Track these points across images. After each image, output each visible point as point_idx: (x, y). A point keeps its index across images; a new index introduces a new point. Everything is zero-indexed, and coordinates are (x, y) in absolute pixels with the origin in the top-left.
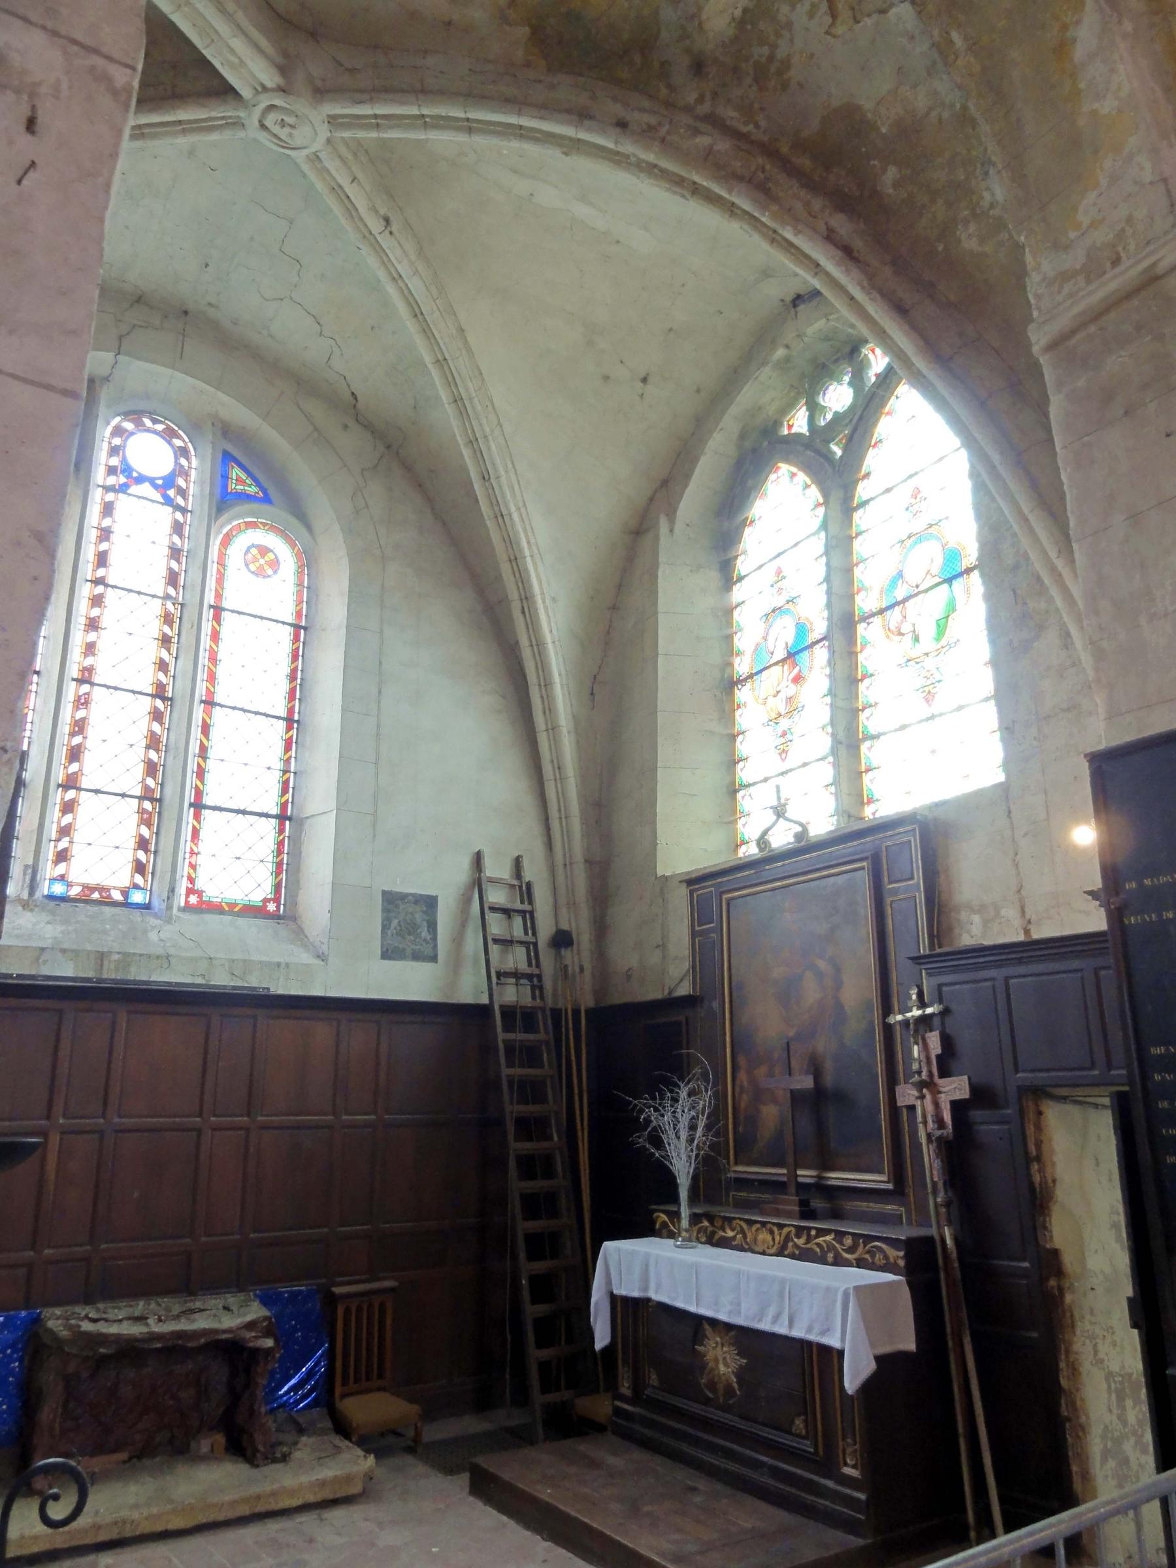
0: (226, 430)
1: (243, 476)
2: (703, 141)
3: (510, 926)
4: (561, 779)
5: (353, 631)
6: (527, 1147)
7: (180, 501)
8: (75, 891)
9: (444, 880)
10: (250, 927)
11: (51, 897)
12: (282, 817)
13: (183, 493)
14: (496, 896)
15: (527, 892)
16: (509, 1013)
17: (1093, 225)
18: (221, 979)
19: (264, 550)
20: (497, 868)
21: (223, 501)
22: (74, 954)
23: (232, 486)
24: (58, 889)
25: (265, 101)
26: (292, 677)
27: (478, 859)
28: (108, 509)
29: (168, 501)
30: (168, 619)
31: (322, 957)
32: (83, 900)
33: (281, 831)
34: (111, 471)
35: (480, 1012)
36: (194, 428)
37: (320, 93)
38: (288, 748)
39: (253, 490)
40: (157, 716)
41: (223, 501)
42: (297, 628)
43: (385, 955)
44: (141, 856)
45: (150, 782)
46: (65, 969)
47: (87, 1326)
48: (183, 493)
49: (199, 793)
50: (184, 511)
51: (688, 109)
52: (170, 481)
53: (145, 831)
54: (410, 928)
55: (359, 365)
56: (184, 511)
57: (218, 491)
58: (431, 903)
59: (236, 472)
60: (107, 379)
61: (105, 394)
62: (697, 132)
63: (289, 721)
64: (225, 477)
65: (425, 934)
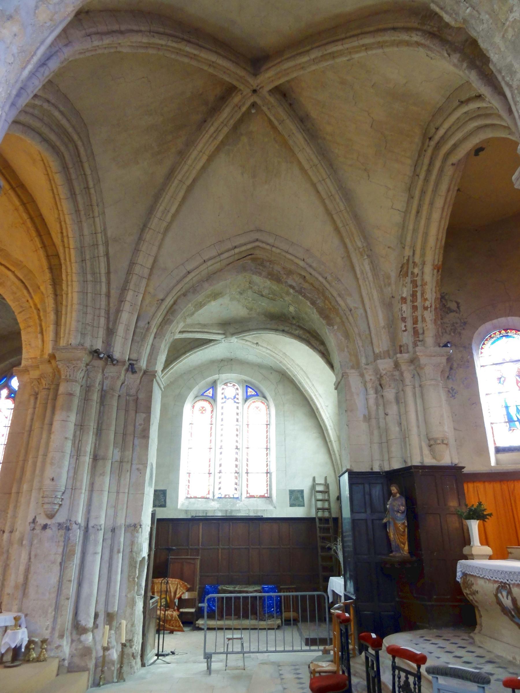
0: (245, 381)
1: (251, 390)
2: (297, 332)
3: (325, 497)
4: (335, 454)
5: (277, 425)
6: (324, 554)
7: (237, 401)
8: (223, 496)
9: (305, 485)
10: (260, 501)
11: (219, 498)
12: (267, 473)
13: (238, 399)
14: (318, 488)
15: (327, 485)
16: (320, 519)
18: (252, 514)
19: (257, 408)
20: (320, 480)
21: (247, 398)
22: (221, 511)
23: (249, 394)
24: (220, 496)
25: (223, 340)
26: (267, 438)
27: (314, 479)
28: (222, 408)
29: (235, 402)
30: (237, 430)
31: (275, 507)
32: (225, 498)
33: (267, 476)
34: (222, 399)
35: (314, 519)
36: (240, 382)
37: (233, 334)
38: (267, 455)
39: (254, 393)
40: (237, 453)
41: (247, 398)
42: (267, 425)
43: (292, 505)
44: (236, 486)
45: (237, 469)
46: (219, 514)
47: (224, 588)
48: (238, 399)
49: (247, 470)
50: (238, 403)
51: (294, 324)
52: (235, 397)
53: (236, 481)
54: (297, 498)
55: (268, 361)
56: (238, 403)
57: (245, 396)
58: (302, 492)
59: (249, 390)
60: (218, 379)
61: (218, 383)
62: (296, 330)
63: (267, 449)
64: (247, 392)
65: (301, 499)
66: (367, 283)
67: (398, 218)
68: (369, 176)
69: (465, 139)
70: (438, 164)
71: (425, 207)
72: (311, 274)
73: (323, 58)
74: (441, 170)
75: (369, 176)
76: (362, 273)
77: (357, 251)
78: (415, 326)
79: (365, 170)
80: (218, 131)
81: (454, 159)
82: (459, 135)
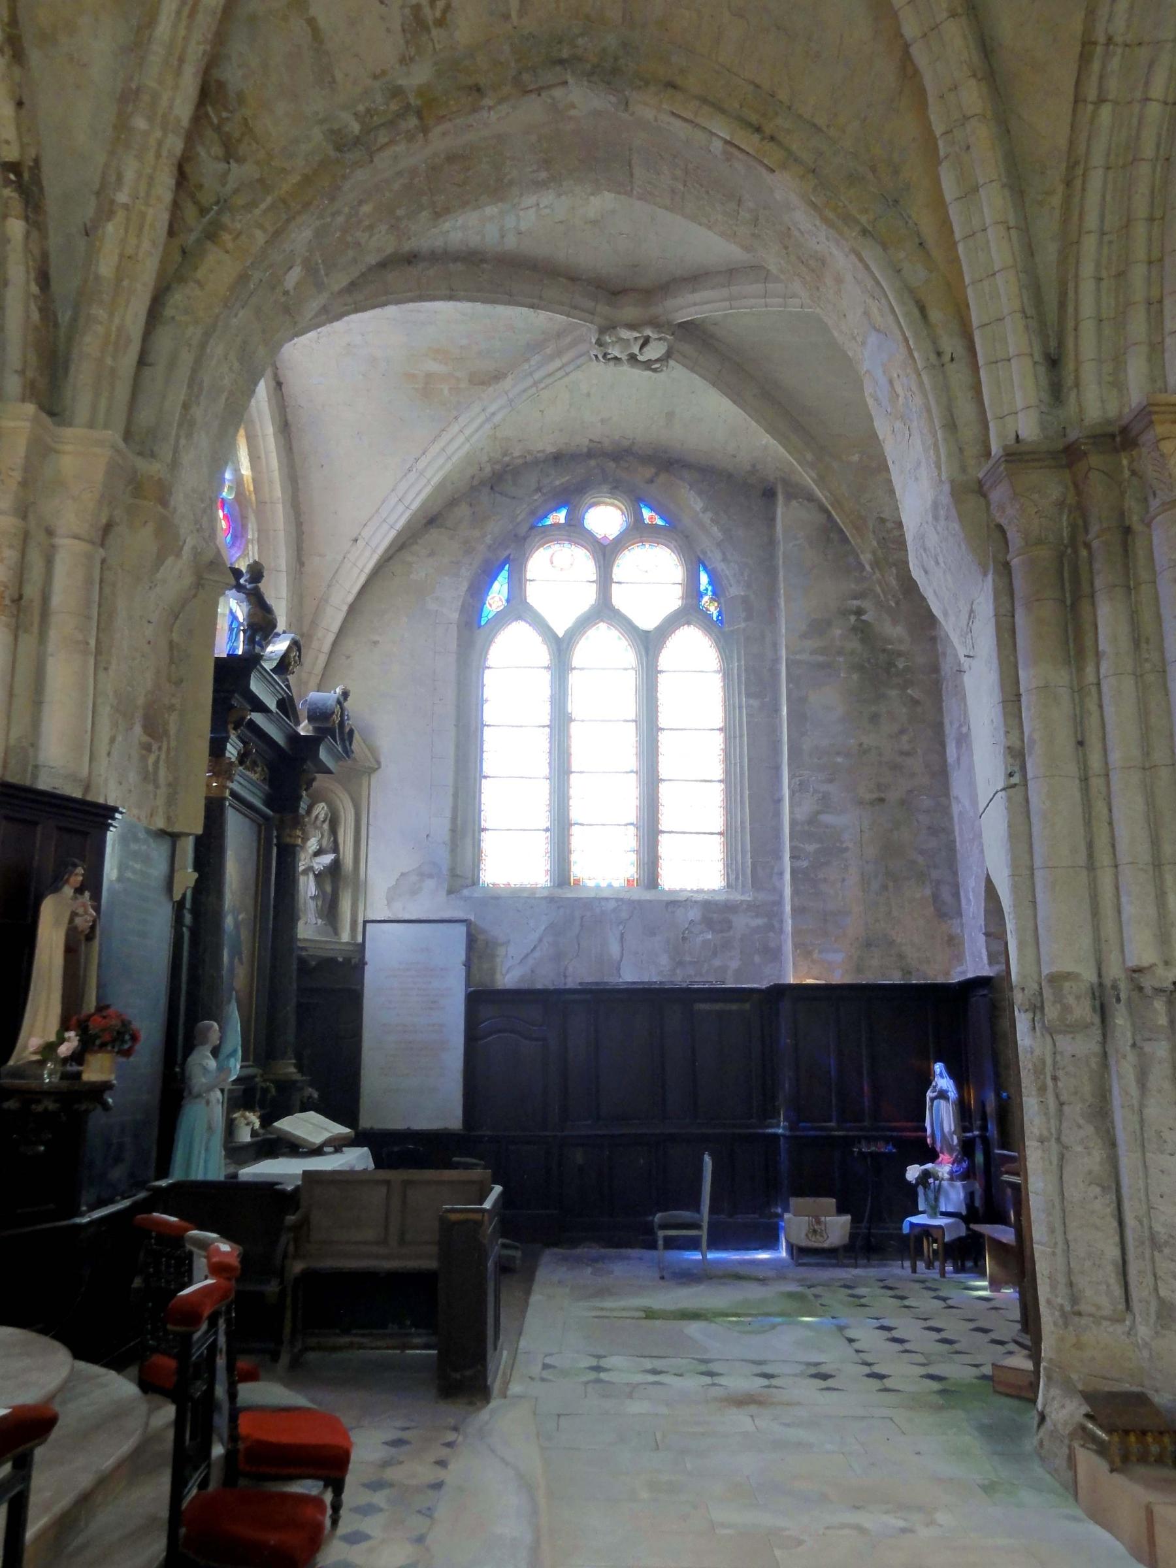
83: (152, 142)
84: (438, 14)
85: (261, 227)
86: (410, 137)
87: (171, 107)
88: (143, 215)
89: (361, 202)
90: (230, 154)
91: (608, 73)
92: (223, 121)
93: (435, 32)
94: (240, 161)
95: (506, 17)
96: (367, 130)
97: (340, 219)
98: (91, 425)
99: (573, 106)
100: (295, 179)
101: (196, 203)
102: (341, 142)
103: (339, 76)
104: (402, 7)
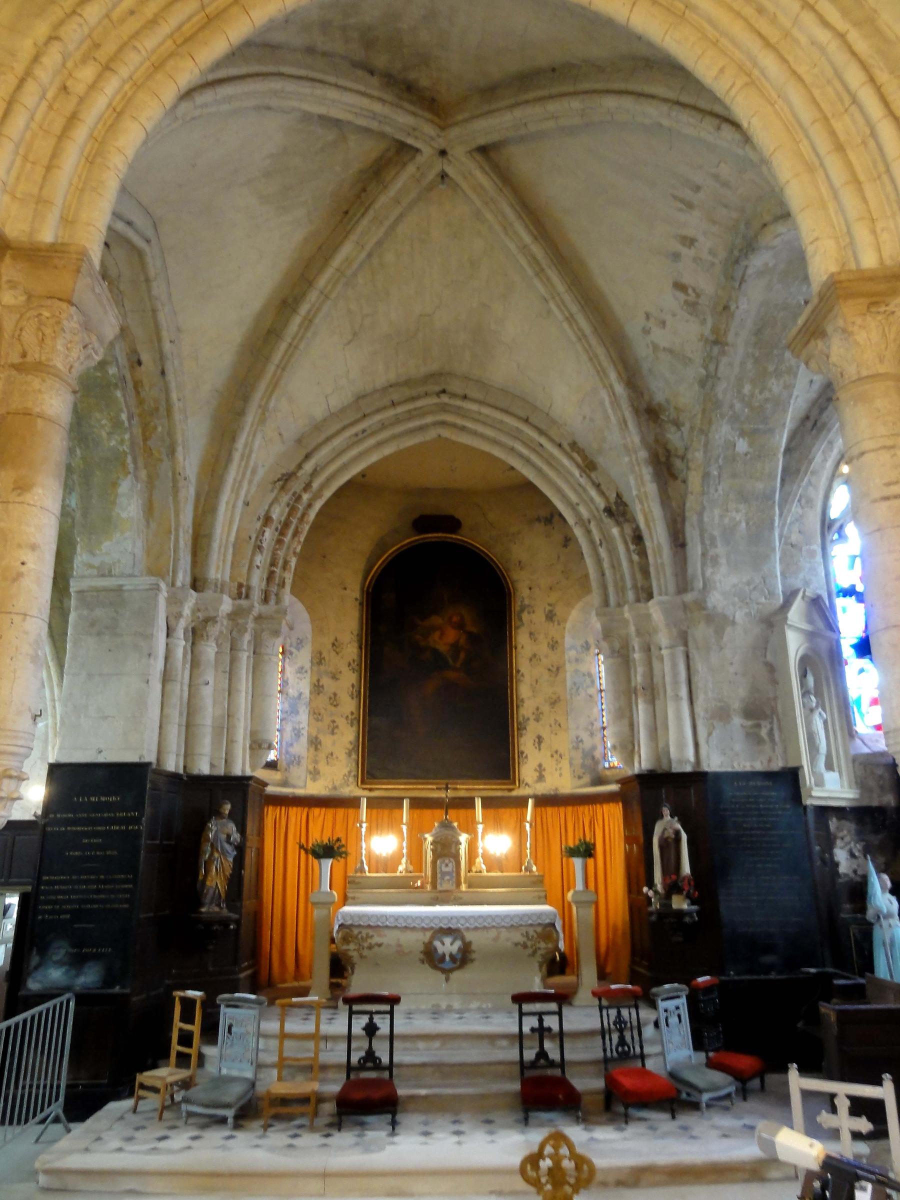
17: (107, 554)
66: (243, 463)
67: (319, 412)
68: (349, 343)
69: (482, 436)
70: (429, 419)
71: (372, 441)
72: (163, 373)
73: (533, 260)
74: (421, 428)
75: (349, 343)
76: (245, 446)
77: (260, 411)
78: (273, 568)
79: (355, 334)
80: (374, 116)
81: (446, 433)
82: (480, 428)
83: (635, 462)
84: (693, 295)
85: (698, 450)
86: (723, 353)
87: (632, 442)
88: (645, 492)
89: (739, 392)
90: (677, 424)
91: (749, 247)
92: (668, 416)
93: (700, 301)
94: (683, 425)
95: (713, 264)
96: (706, 367)
97: (738, 406)
98: (660, 594)
99: (766, 264)
100: (699, 416)
101: (678, 457)
102: (703, 383)
103: (691, 356)
104: (682, 308)
